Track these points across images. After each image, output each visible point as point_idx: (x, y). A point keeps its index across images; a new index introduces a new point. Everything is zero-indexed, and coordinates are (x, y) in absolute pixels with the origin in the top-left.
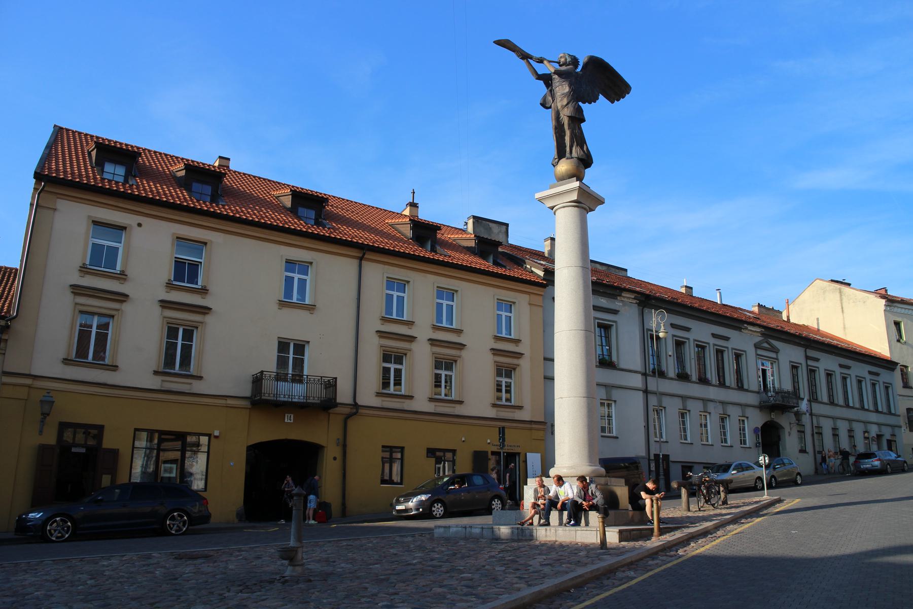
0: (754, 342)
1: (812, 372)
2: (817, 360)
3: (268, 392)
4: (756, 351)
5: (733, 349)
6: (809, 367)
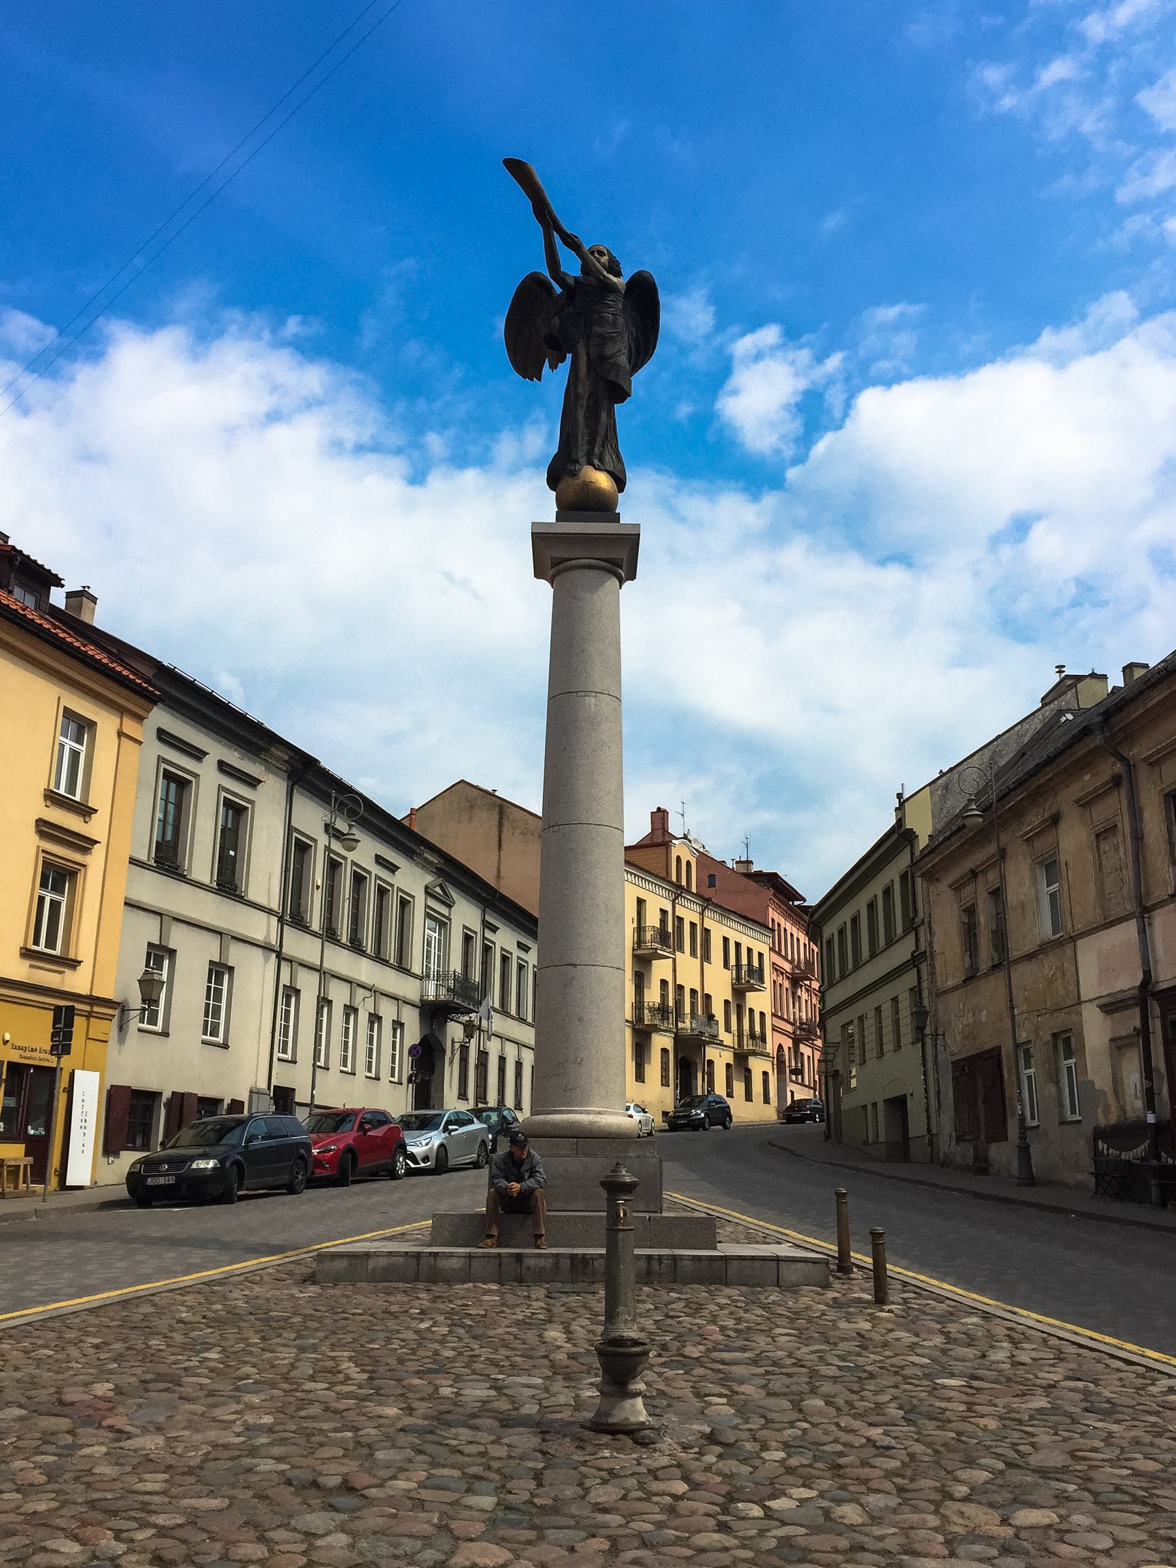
0: (425, 883)
1: (487, 949)
2: (494, 929)
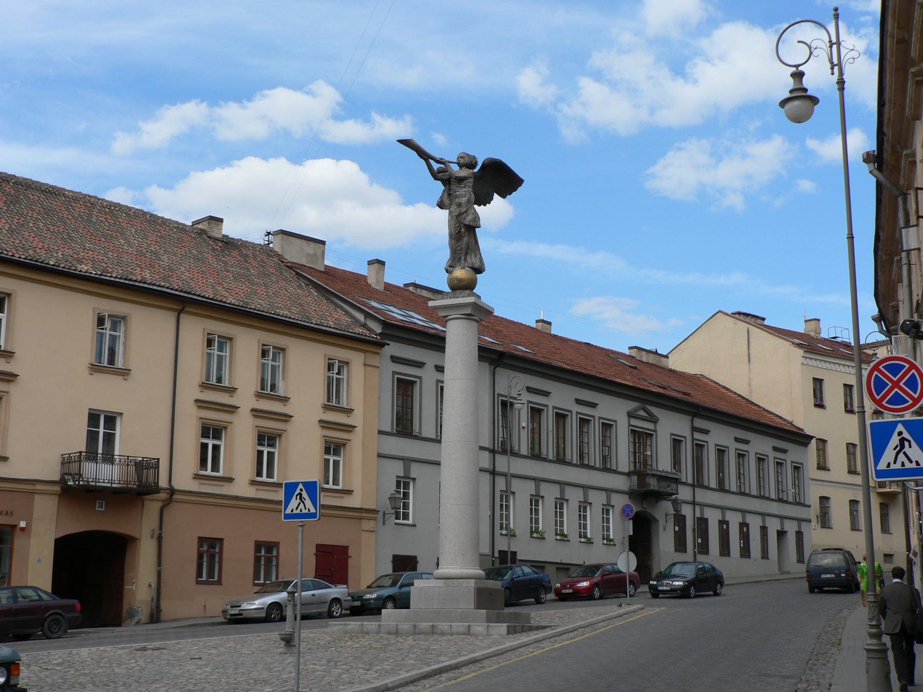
0: (627, 410)
1: (699, 447)
2: (706, 432)
3: (103, 478)
4: (629, 421)
5: (600, 418)
6: (758, 456)
